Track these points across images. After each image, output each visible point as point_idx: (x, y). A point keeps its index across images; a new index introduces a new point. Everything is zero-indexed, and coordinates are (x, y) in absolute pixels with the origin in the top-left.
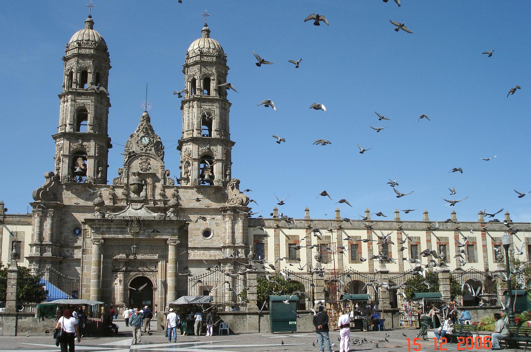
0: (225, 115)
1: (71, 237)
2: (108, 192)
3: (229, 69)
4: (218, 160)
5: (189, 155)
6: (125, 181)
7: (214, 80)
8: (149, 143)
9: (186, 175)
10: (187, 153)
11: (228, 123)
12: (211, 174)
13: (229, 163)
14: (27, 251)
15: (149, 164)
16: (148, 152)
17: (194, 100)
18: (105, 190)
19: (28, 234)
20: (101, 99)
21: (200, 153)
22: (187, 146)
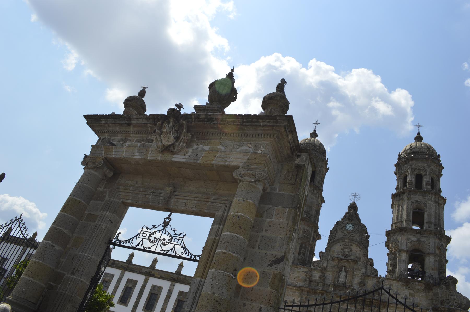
0: (439, 210)
2: (305, 274)
3: (443, 168)
4: (429, 254)
5: (397, 246)
6: (325, 265)
7: (426, 175)
8: (354, 229)
9: (391, 268)
10: (394, 244)
11: (443, 219)
12: (421, 270)
13: (444, 261)
15: (351, 251)
16: (352, 238)
17: (403, 193)
18: (303, 271)
20: (313, 190)
21: (409, 245)
22: (395, 237)
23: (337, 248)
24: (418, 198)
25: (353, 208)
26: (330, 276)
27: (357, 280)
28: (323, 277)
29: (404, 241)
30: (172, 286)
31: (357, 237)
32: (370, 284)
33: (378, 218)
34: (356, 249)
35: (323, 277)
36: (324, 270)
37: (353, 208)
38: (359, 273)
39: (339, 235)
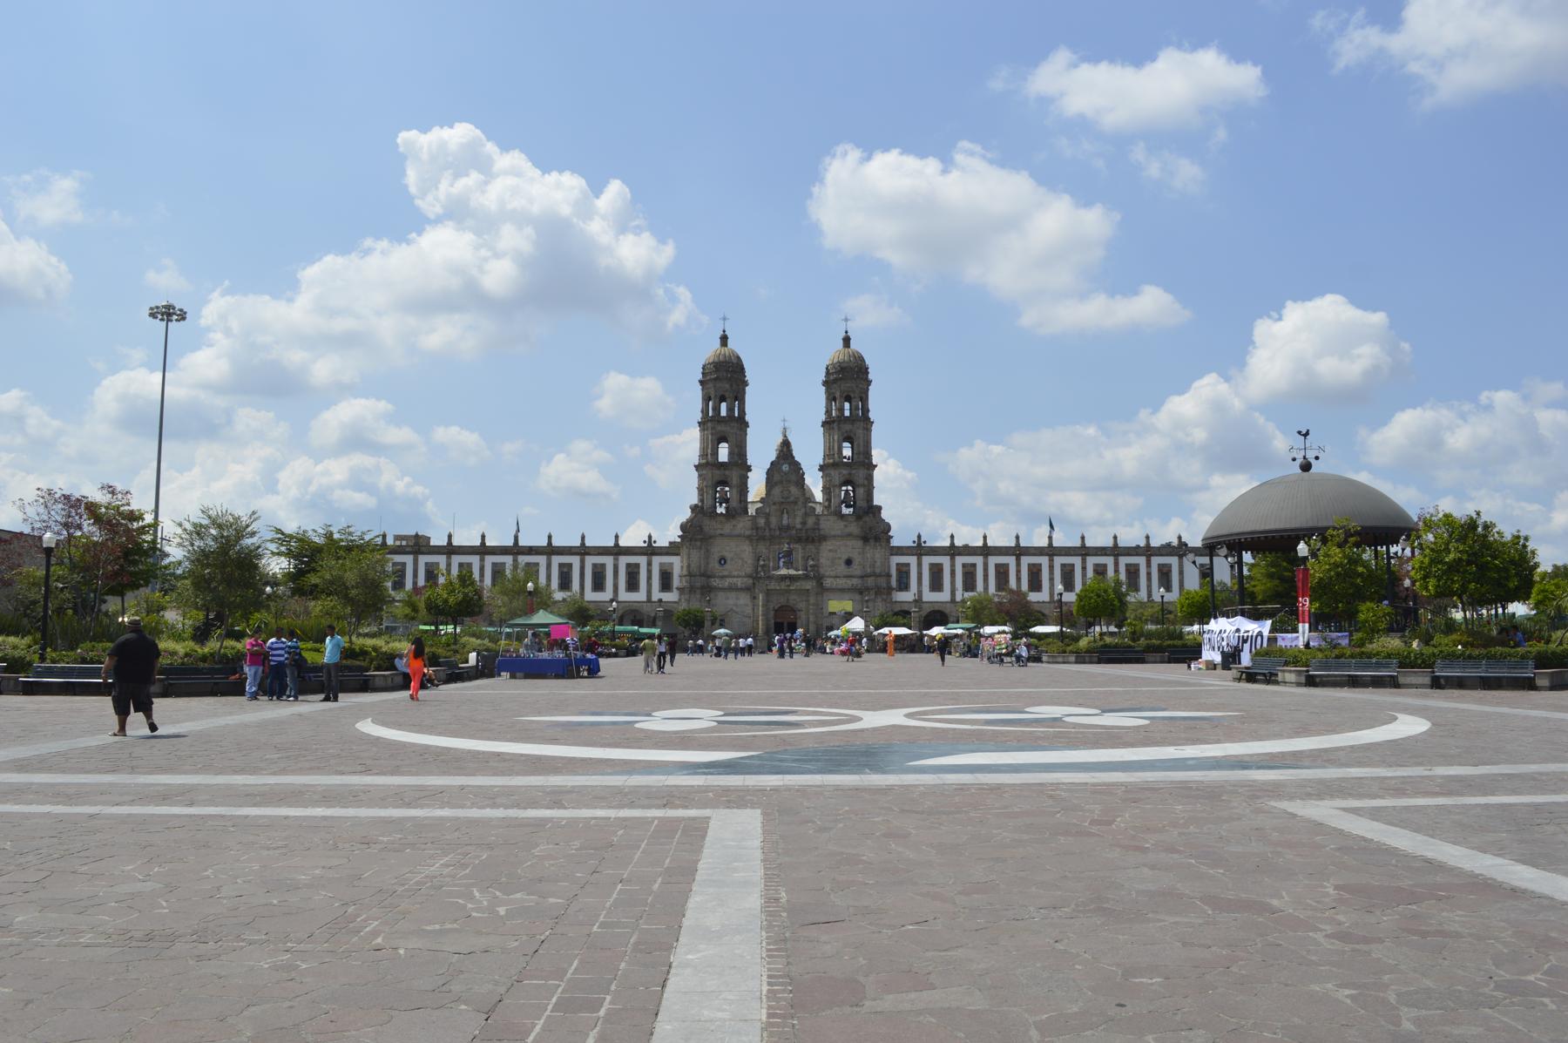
1: (717, 565)
14: (676, 582)
19: (677, 563)
23: (777, 491)
24: (847, 427)
25: (786, 445)
26: (773, 520)
27: (798, 520)
28: (768, 523)
29: (837, 476)
30: (616, 560)
31: (793, 478)
32: (811, 521)
33: (810, 454)
34: (794, 490)
35: (768, 523)
36: (767, 516)
37: (786, 445)
38: (800, 513)
39: (777, 477)
